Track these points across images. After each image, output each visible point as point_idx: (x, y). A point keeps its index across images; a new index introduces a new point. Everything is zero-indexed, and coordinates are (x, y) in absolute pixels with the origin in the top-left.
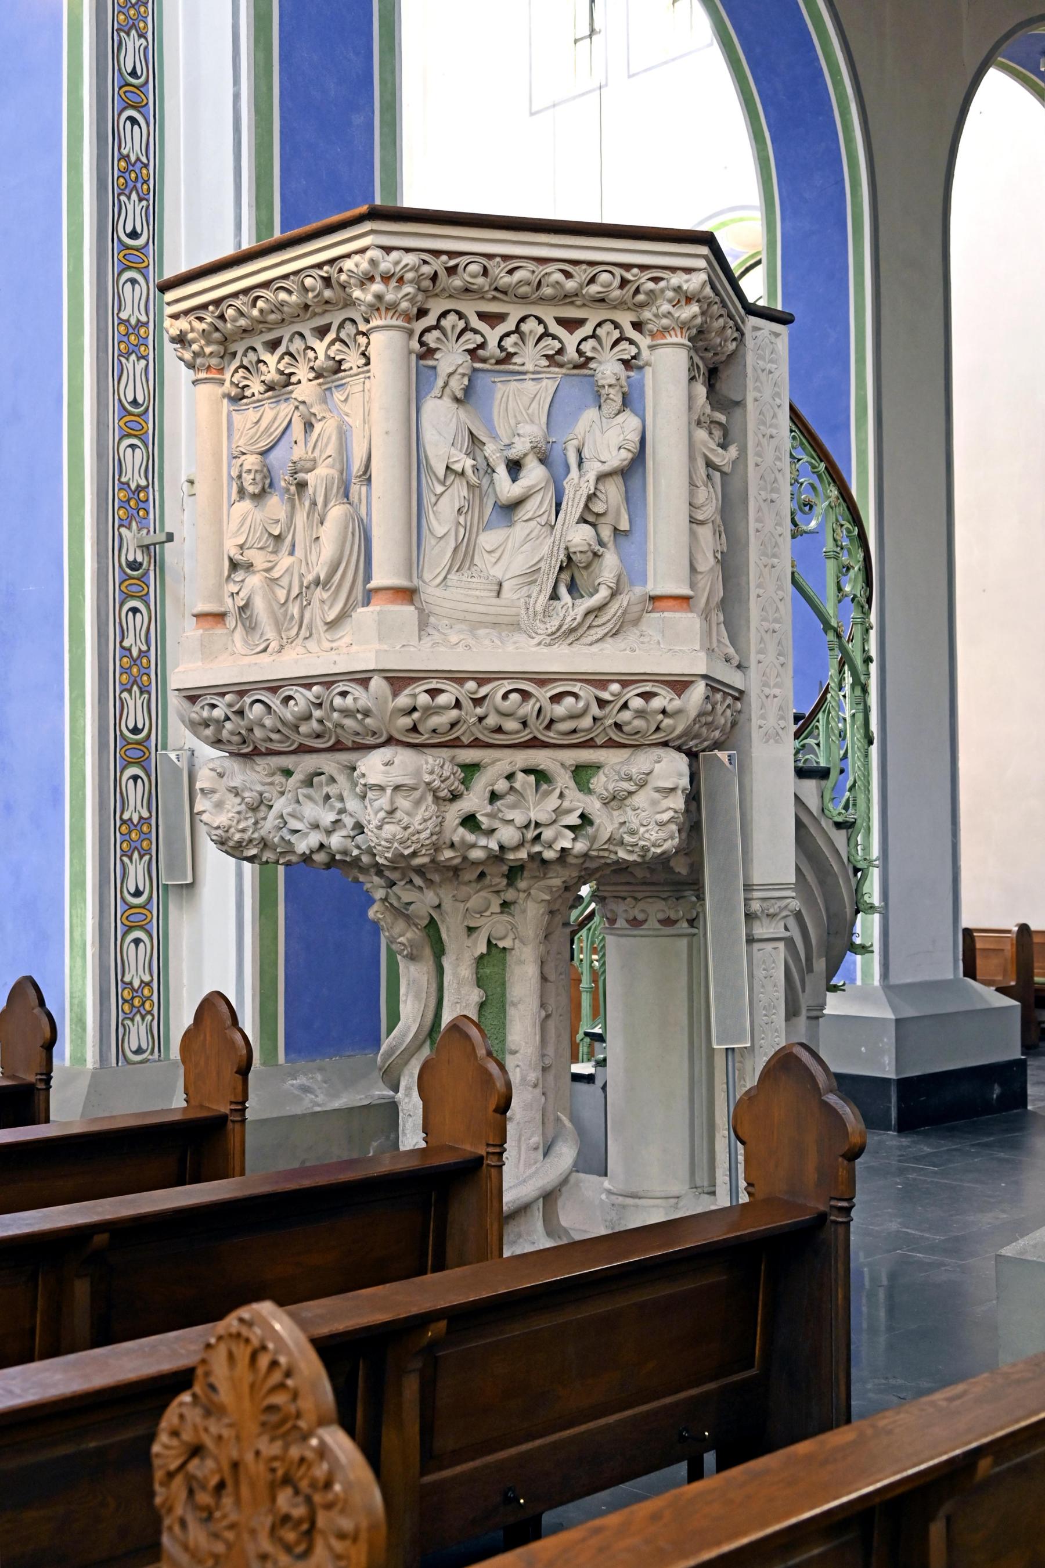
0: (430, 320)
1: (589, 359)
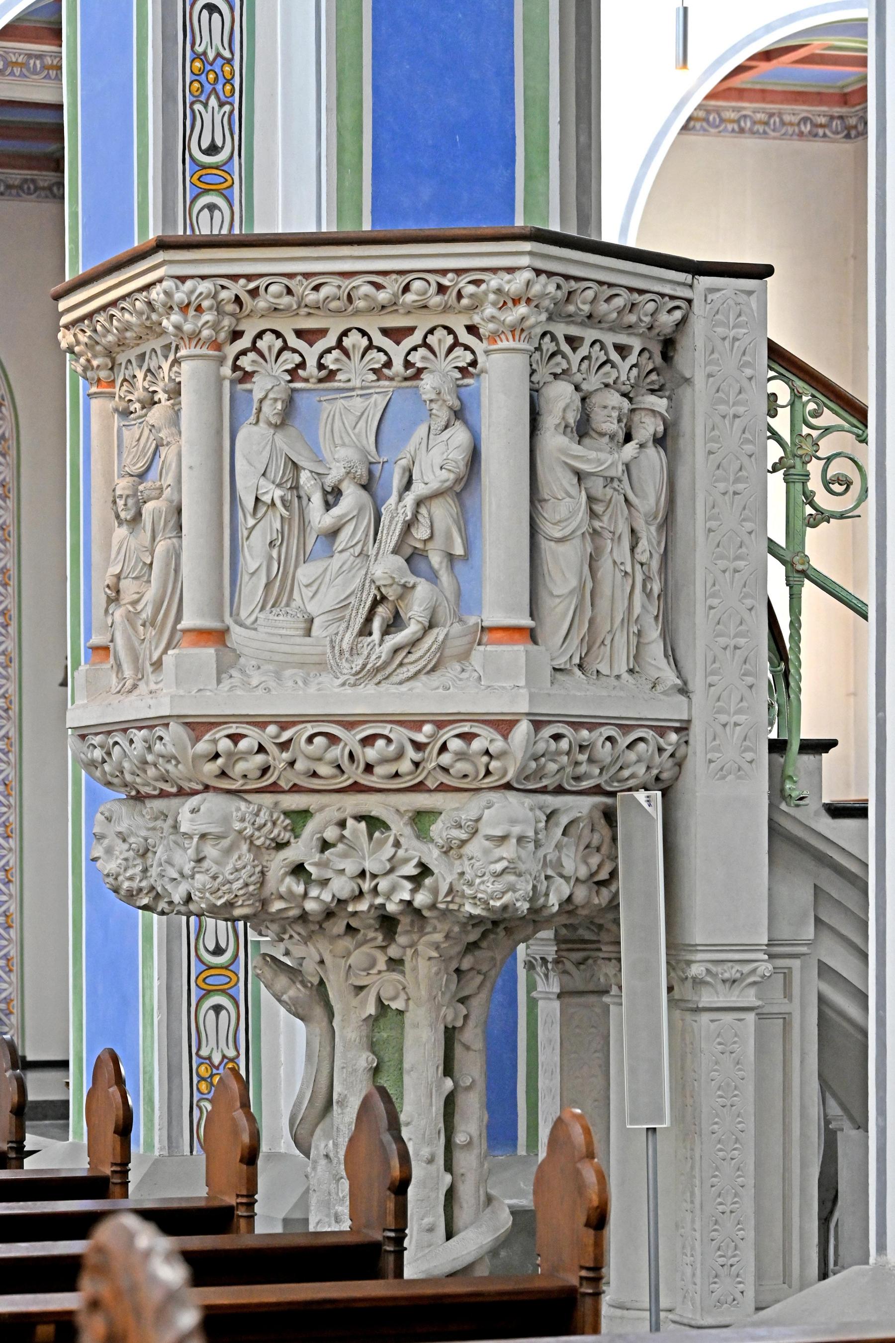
0: (244, 342)
1: (420, 371)
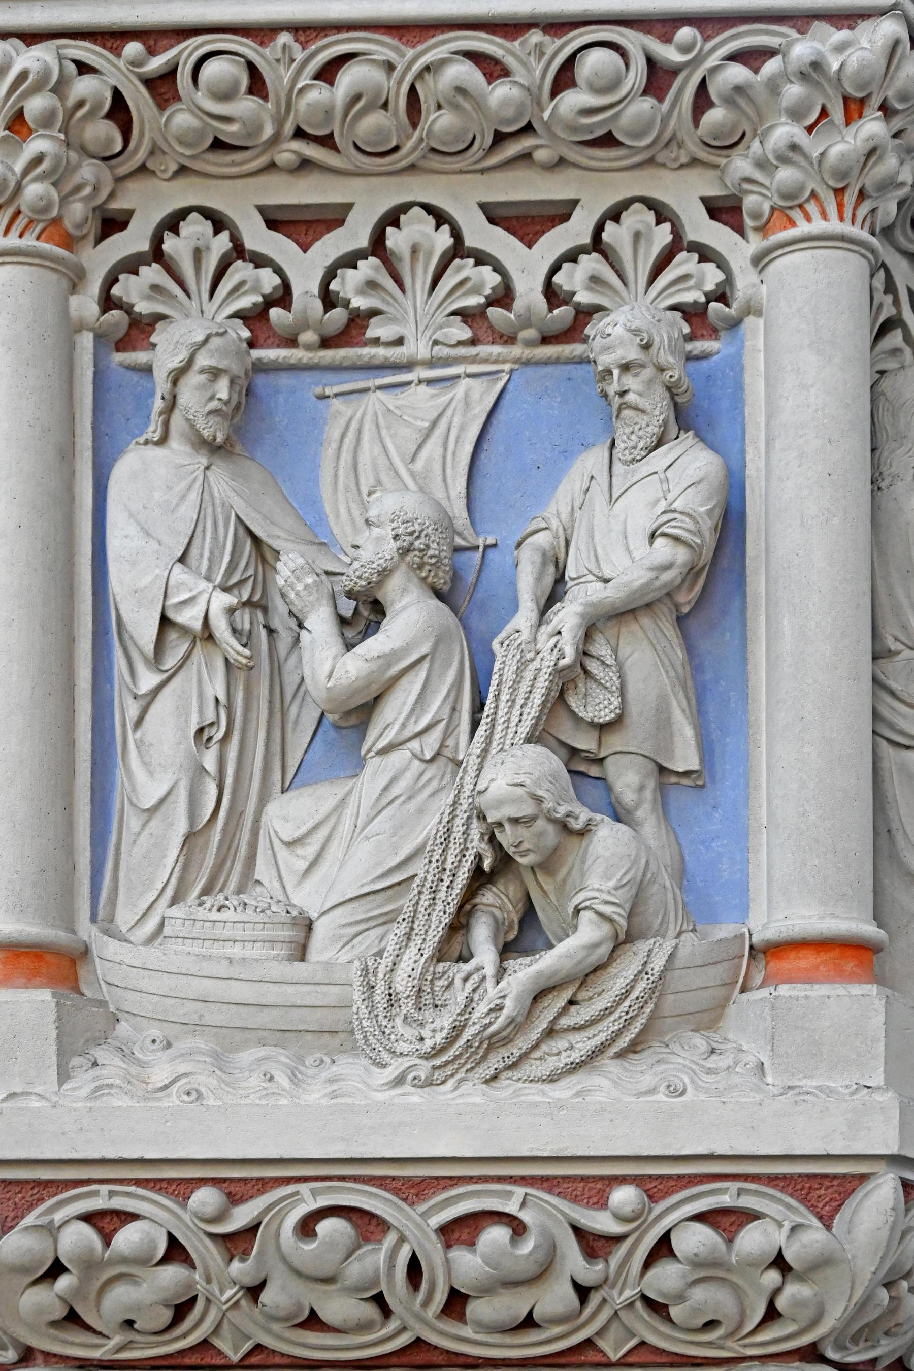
0: (133, 240)
1: (586, 314)
